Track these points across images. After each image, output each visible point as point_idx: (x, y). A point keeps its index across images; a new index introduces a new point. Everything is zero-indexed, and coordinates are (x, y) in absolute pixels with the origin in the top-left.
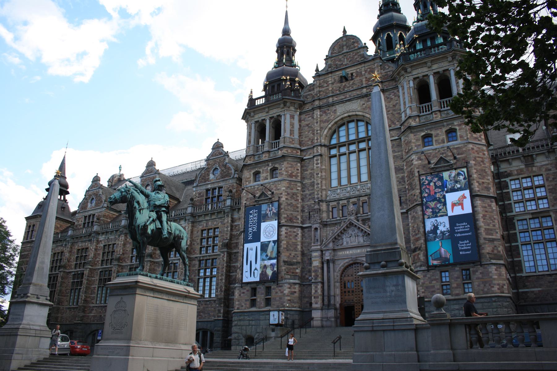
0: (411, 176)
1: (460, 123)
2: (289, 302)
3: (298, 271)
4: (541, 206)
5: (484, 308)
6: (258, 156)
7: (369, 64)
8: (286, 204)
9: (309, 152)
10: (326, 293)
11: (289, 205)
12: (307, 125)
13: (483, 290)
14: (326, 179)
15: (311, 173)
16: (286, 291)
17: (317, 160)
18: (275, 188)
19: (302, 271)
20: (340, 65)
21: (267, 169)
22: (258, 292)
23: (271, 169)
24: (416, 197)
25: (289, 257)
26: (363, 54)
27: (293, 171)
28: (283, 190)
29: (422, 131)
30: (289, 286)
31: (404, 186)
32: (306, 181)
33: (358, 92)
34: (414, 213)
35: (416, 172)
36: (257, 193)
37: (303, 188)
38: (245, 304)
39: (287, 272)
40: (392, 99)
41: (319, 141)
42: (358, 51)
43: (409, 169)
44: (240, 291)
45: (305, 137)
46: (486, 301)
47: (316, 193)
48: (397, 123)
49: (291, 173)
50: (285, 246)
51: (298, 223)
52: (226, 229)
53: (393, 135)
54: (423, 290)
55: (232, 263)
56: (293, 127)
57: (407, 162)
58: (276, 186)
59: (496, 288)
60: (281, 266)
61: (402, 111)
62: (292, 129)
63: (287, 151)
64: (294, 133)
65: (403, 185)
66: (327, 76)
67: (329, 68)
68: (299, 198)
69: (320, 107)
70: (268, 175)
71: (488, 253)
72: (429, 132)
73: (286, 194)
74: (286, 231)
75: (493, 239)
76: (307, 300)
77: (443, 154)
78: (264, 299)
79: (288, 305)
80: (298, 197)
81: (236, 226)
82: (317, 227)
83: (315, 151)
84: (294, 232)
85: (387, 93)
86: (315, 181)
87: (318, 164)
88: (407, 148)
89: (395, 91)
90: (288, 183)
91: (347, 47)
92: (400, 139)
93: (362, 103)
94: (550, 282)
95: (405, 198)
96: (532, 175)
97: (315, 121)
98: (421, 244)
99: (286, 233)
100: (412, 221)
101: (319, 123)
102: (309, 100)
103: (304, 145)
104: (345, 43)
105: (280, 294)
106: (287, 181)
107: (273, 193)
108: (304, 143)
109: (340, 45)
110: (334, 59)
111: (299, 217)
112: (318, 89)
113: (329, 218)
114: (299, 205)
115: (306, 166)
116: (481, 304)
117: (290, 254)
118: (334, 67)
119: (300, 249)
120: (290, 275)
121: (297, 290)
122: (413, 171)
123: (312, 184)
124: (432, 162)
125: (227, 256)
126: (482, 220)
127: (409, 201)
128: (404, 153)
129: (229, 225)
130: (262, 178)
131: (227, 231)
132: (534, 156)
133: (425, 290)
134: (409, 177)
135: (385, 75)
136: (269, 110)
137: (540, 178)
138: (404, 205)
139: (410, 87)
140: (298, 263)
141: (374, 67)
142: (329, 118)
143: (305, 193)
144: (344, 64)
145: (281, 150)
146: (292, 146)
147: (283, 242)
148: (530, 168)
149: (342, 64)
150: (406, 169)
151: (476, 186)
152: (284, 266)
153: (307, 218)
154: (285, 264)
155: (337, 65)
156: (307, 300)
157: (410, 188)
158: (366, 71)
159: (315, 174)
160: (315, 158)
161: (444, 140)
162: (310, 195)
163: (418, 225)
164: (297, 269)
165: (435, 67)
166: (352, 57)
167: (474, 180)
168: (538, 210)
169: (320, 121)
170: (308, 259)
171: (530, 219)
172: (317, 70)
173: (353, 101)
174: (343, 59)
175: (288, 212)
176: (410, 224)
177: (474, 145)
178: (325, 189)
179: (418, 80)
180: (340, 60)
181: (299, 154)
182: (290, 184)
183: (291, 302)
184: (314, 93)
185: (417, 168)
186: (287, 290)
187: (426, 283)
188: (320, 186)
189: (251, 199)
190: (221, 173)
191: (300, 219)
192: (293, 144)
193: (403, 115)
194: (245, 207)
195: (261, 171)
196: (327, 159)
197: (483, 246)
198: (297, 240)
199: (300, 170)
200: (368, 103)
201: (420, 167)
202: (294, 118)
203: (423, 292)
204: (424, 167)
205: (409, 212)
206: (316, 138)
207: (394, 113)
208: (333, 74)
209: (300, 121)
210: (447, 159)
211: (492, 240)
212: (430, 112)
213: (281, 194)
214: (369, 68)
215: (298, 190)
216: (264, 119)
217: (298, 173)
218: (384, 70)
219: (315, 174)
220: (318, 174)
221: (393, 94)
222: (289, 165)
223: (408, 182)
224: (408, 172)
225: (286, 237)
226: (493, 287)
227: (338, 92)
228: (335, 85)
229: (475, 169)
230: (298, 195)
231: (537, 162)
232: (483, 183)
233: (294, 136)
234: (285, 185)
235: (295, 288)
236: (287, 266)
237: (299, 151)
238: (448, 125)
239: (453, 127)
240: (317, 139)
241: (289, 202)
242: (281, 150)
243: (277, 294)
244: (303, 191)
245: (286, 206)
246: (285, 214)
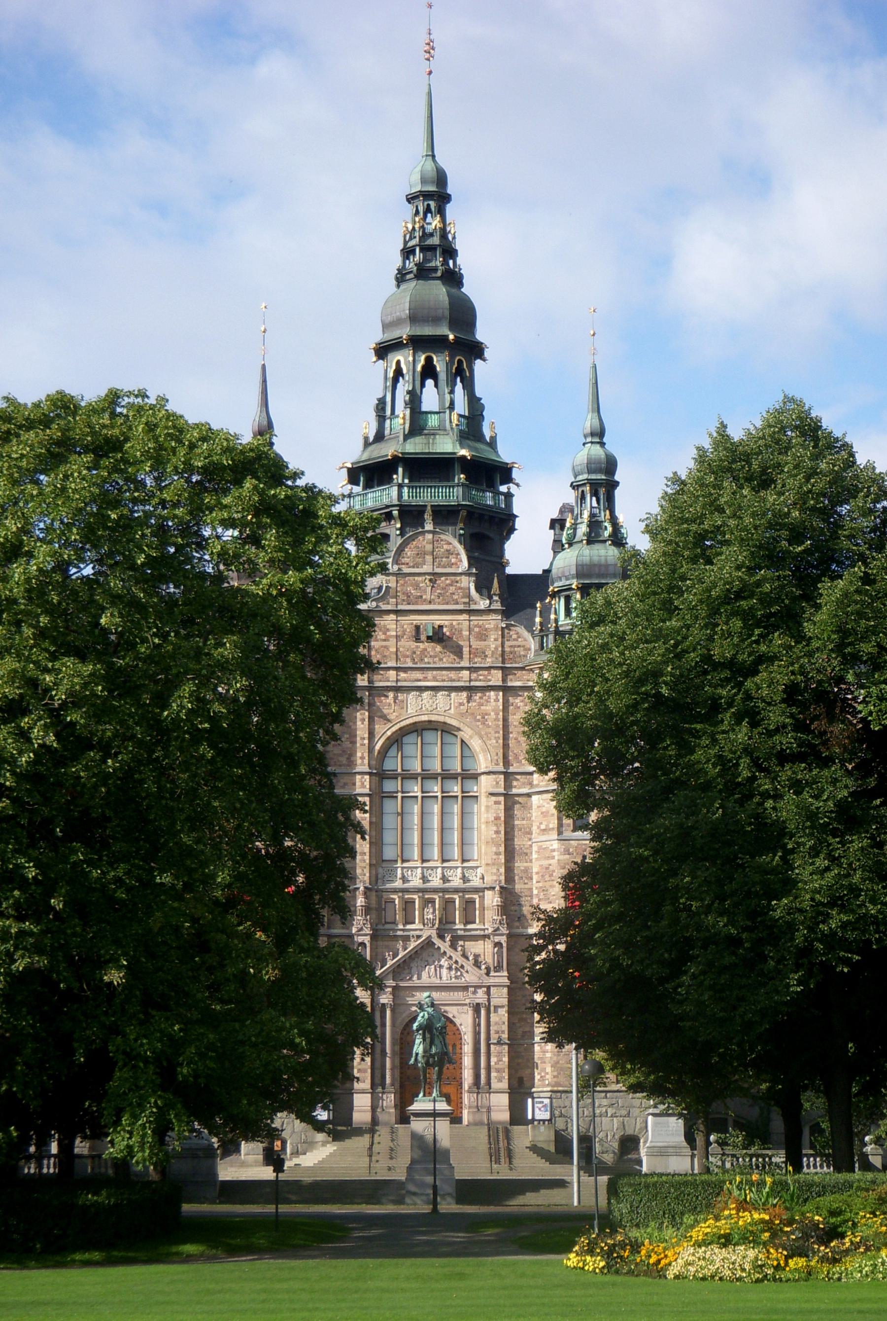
0: (547, 878)
33: (452, 675)
43: (545, 863)
57: (540, 848)
88: (545, 823)
133: (559, 1074)
134: (542, 876)
180: (417, 586)
223: (540, 884)
227: (408, 660)
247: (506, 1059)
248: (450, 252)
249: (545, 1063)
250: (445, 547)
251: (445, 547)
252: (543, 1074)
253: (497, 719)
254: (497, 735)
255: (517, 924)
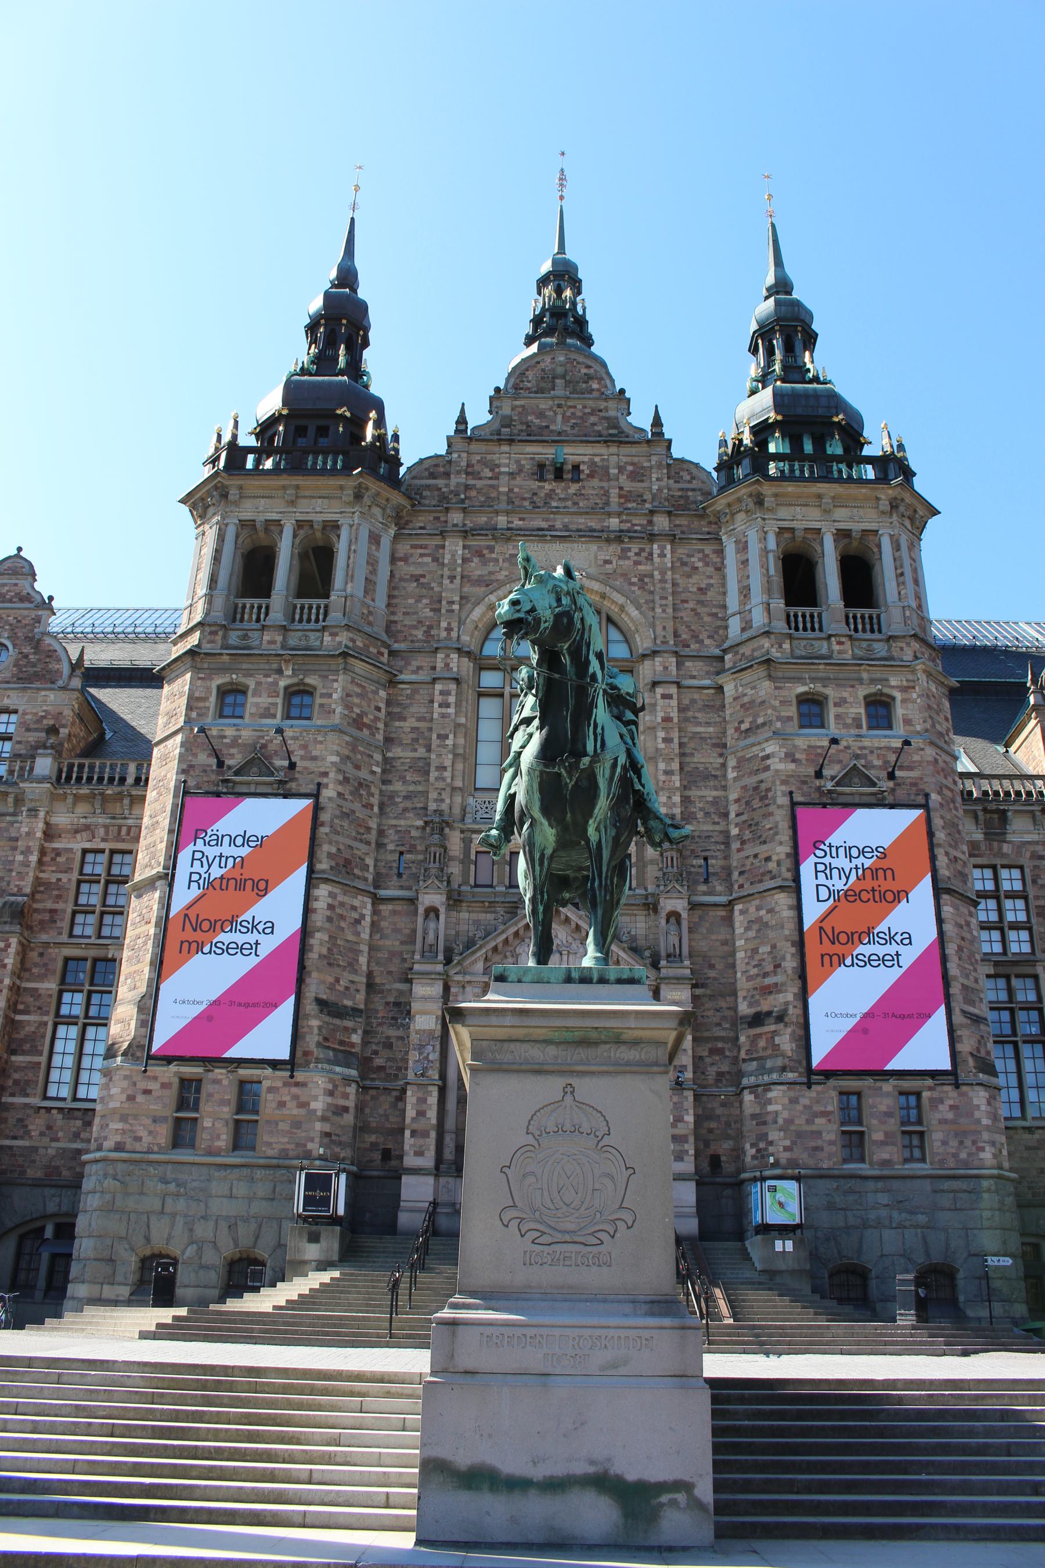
0: (756, 803)
1: (905, 683)
2: (326, 1140)
3: (356, 1038)
4: (1014, 948)
5: (958, 1206)
6: (240, 633)
7: (633, 450)
8: (338, 813)
9: (415, 664)
10: (450, 1123)
11: (345, 815)
12: (416, 578)
13: (955, 1155)
14: (465, 759)
15: (417, 729)
16: (318, 1105)
17: (444, 693)
18: (302, 752)
19: (365, 1043)
20: (541, 428)
21: (275, 684)
22: (210, 1095)
23: (286, 688)
24: (772, 865)
25: (331, 987)
26: (617, 418)
27: (366, 709)
28: (332, 763)
29: (800, 680)
30: (330, 1087)
31: (717, 828)
32: (396, 752)
34: (763, 912)
35: (779, 793)
36: (232, 756)
37: (384, 771)
38: (150, 1133)
39: (326, 1039)
40: (697, 568)
41: (454, 634)
42: (603, 405)
43: (751, 781)
44: (135, 1084)
45: (404, 614)
46: (965, 1187)
47: (433, 795)
48: (707, 642)
49: (360, 716)
50: (325, 951)
51: (366, 879)
52: (20, 858)
53: (695, 673)
54: (787, 1143)
55: (28, 980)
56: (374, 572)
58: (305, 747)
59: (987, 1155)
60: (307, 1016)
61: (729, 612)
62: (370, 577)
63: (353, 640)
64: (374, 591)
65: (715, 823)
66: (496, 449)
67: (503, 426)
68: (375, 801)
69: (466, 533)
70: (276, 704)
71: (971, 1054)
72: (819, 688)
73: (341, 778)
74: (330, 901)
75: (975, 1015)
76: (373, 1138)
77: (857, 757)
78: (231, 1125)
79: (321, 1151)
80: (373, 795)
81: (58, 853)
82: (437, 904)
83: (440, 665)
84: (354, 908)
85: (682, 551)
86: (433, 756)
87: (448, 705)
89: (708, 549)
90: (347, 743)
91: (568, 383)
92: (720, 689)
93: (602, 556)
94: (1028, 1148)
95: (721, 862)
96: (999, 862)
97: (446, 572)
98: (787, 1003)
99: (331, 907)
100: (751, 934)
101: (458, 580)
102: (427, 502)
103: (400, 637)
104: (560, 370)
105: (295, 1111)
106: (347, 738)
107: (292, 766)
108: (402, 632)
109: (543, 370)
110: (523, 406)
111: (370, 861)
112: (462, 479)
113: (466, 882)
114: (373, 824)
115: (399, 704)
116: (951, 1195)
117: (337, 980)
118: (519, 427)
119: (365, 968)
120: (334, 1049)
121: (351, 1103)
122: (768, 790)
123: (423, 769)
124: (825, 772)
125: (17, 953)
126: (955, 959)
127: (741, 873)
128: (730, 731)
129: (35, 845)
130: (254, 710)
131: (26, 864)
132: (1009, 814)
133: (794, 1143)
134: (747, 803)
135: (680, 497)
136: (297, 497)
137: (1016, 873)
138: (716, 883)
139: (767, 552)
140: (356, 1012)
141: (646, 464)
142: (491, 573)
143: (391, 788)
144: (552, 428)
145: (333, 635)
146: (367, 629)
147: (318, 935)
148: (995, 844)
149: (547, 427)
150: (735, 779)
151: (944, 865)
152: (316, 1017)
153: (391, 868)
154: (321, 1011)
155: (528, 426)
156: (373, 1138)
157: (747, 834)
158: (621, 469)
159: (434, 736)
160: (438, 687)
161: (861, 719)
162: (406, 798)
163: (774, 947)
164: (355, 1031)
165: (840, 513)
166: (581, 418)
167: (939, 845)
168: (1010, 957)
169: (462, 577)
170: (387, 1003)
171: (988, 976)
172: (462, 420)
173: (576, 545)
174: (551, 413)
175: (340, 839)
176: (740, 943)
177: (939, 752)
178: (460, 789)
179: (787, 535)
180: (541, 415)
181: (385, 659)
182: (354, 750)
183: (333, 1142)
184: (448, 485)
185: (784, 782)
186: (321, 1098)
187: (797, 1122)
188: (447, 774)
189: (205, 771)
190: (16, 665)
191: (371, 869)
192: (370, 624)
193: (735, 626)
194: (185, 793)
195: (252, 685)
196: (471, 695)
197: (959, 1033)
198: (358, 934)
199: (383, 711)
200: (621, 563)
201: (792, 780)
202: (378, 544)
203: (786, 1149)
204: (805, 782)
205: (738, 908)
206: (444, 624)
207: (699, 611)
208: (517, 448)
209: (393, 559)
210: (872, 774)
211: (977, 1020)
212: (823, 635)
213: (325, 774)
214: (632, 464)
215: (373, 773)
216: (278, 523)
217: (377, 719)
218: (676, 482)
219: (434, 736)
220: (447, 737)
221: (700, 555)
222: (358, 690)
223: (744, 817)
224: (744, 788)
225: (329, 919)
226: (982, 1149)
227: (526, 503)
228: (519, 481)
229: (942, 817)
230: (373, 789)
231: (1014, 833)
232: (955, 857)
233: (373, 600)
234: (339, 749)
235: (346, 1096)
236: (327, 1019)
237: (386, 651)
238: (873, 681)
239: (886, 690)
240: (449, 630)
241: (347, 806)
242: (333, 635)
243: (285, 1112)
244: (385, 782)
245: (336, 817)
246: (330, 843)
247: (690, 1118)
248: (581, 322)
249: (764, 1123)
250: (584, 371)
251: (584, 371)
252: (762, 1145)
253: (663, 581)
254: (664, 602)
255: (703, 888)
